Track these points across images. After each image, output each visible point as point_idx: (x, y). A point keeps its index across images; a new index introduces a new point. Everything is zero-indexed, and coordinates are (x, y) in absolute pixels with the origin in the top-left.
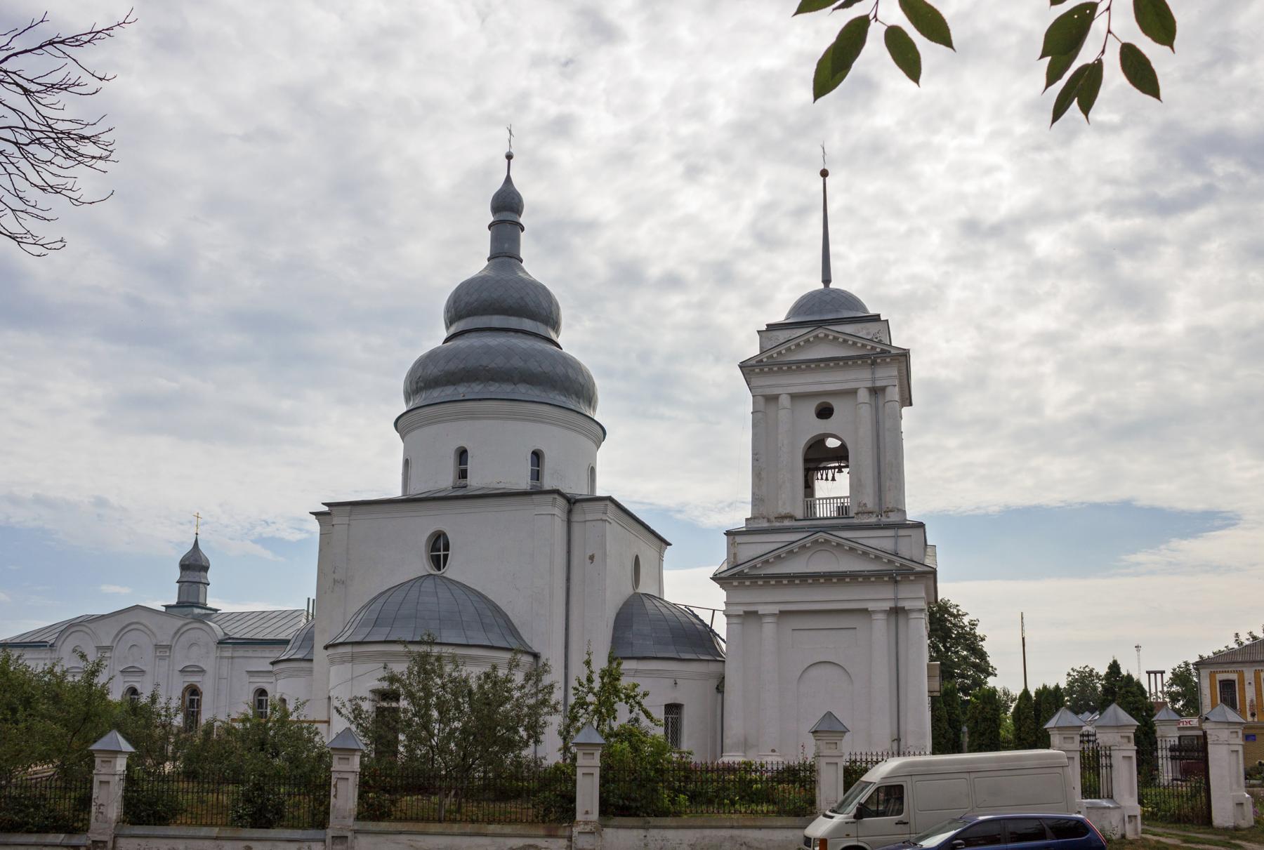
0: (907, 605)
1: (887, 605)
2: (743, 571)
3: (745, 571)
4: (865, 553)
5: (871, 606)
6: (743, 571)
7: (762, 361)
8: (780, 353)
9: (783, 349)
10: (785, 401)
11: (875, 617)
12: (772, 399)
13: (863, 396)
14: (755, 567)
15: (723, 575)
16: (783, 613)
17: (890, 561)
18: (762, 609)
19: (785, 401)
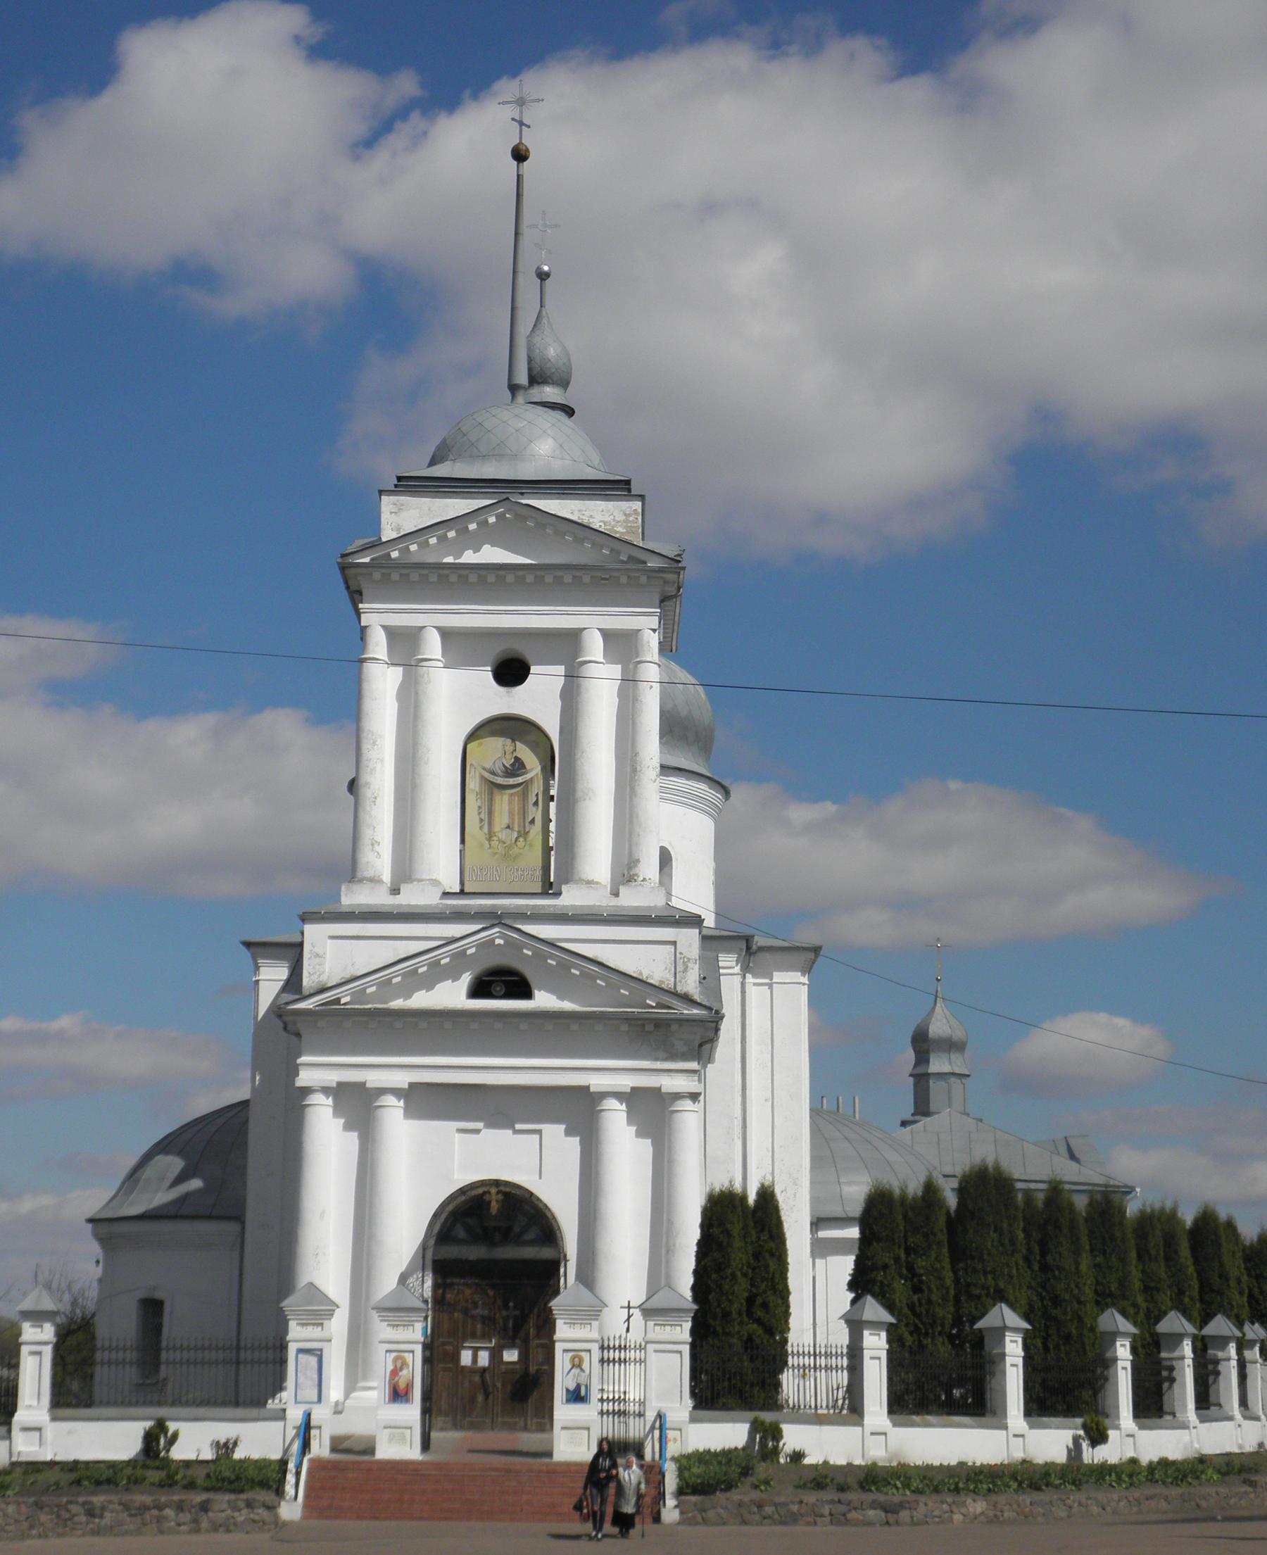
6: (339, 999)
19: (433, 646)
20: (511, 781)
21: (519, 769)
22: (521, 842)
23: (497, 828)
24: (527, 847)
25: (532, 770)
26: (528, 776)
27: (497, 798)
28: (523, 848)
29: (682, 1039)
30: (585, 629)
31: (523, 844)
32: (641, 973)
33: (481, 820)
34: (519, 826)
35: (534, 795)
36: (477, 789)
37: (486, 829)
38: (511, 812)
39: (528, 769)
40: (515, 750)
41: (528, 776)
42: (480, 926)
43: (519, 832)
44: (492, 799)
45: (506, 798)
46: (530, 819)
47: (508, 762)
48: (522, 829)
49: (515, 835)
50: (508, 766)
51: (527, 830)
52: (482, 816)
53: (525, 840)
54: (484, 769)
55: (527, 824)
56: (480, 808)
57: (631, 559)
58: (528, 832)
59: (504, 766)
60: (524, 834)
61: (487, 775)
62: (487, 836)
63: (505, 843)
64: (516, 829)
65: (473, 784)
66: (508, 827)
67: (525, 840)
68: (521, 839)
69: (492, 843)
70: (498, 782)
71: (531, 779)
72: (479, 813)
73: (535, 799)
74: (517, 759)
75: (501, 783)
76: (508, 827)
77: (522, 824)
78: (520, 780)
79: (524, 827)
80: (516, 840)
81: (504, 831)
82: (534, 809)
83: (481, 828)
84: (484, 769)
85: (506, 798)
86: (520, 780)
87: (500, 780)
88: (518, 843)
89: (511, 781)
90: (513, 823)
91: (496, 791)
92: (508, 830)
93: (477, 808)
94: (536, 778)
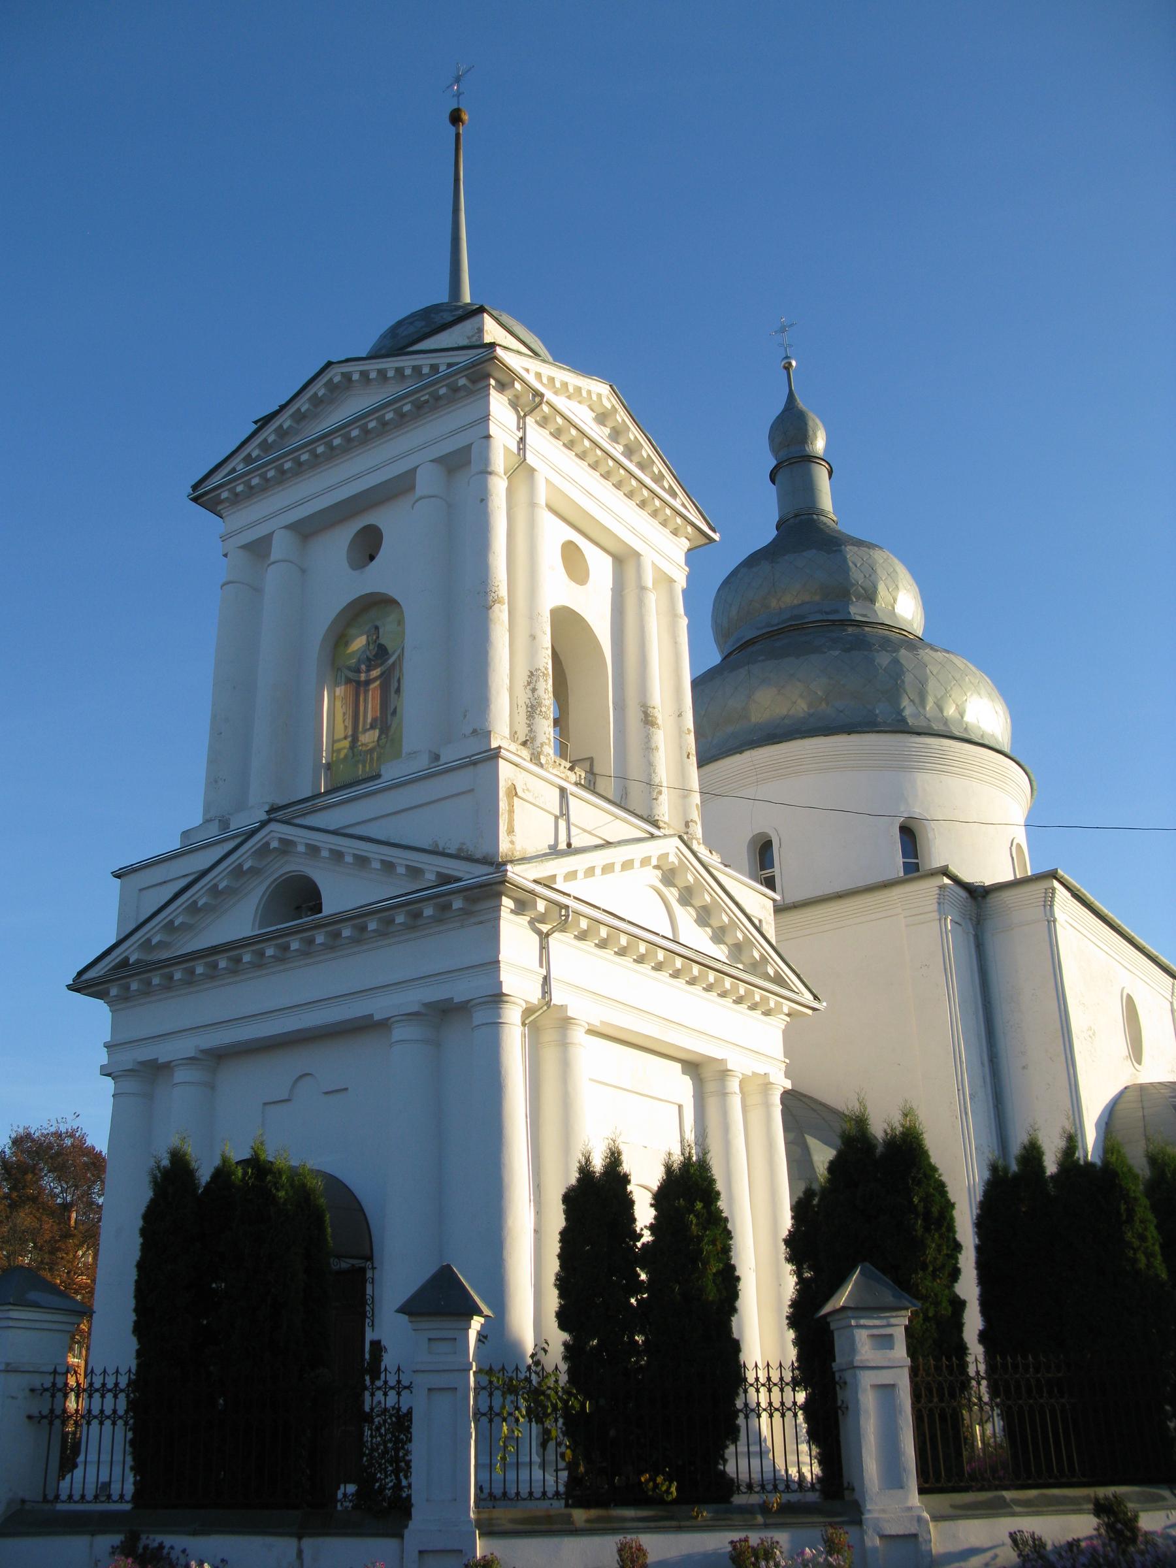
0: (460, 990)
1: (412, 999)
2: (127, 959)
4: (362, 861)
5: (378, 1007)
6: (127, 959)
7: (234, 470)
8: (265, 446)
9: (269, 434)
10: (282, 545)
11: (398, 1033)
12: (259, 549)
13: (428, 480)
14: (147, 945)
15: (91, 974)
16: (219, 1057)
17: (415, 872)
18: (164, 1052)
19: (282, 545)
25: (394, 653)
26: (391, 661)
30: (418, 467)
32: (437, 845)
35: (396, 679)
36: (342, 694)
39: (390, 651)
40: (378, 637)
46: (392, 709)
52: (347, 724)
53: (387, 737)
55: (389, 717)
56: (344, 714)
57: (450, 365)
58: (391, 724)
67: (387, 737)
68: (383, 736)
71: (394, 664)
72: (344, 722)
73: (396, 684)
79: (387, 718)
88: (381, 742)
93: (341, 715)
94: (398, 662)
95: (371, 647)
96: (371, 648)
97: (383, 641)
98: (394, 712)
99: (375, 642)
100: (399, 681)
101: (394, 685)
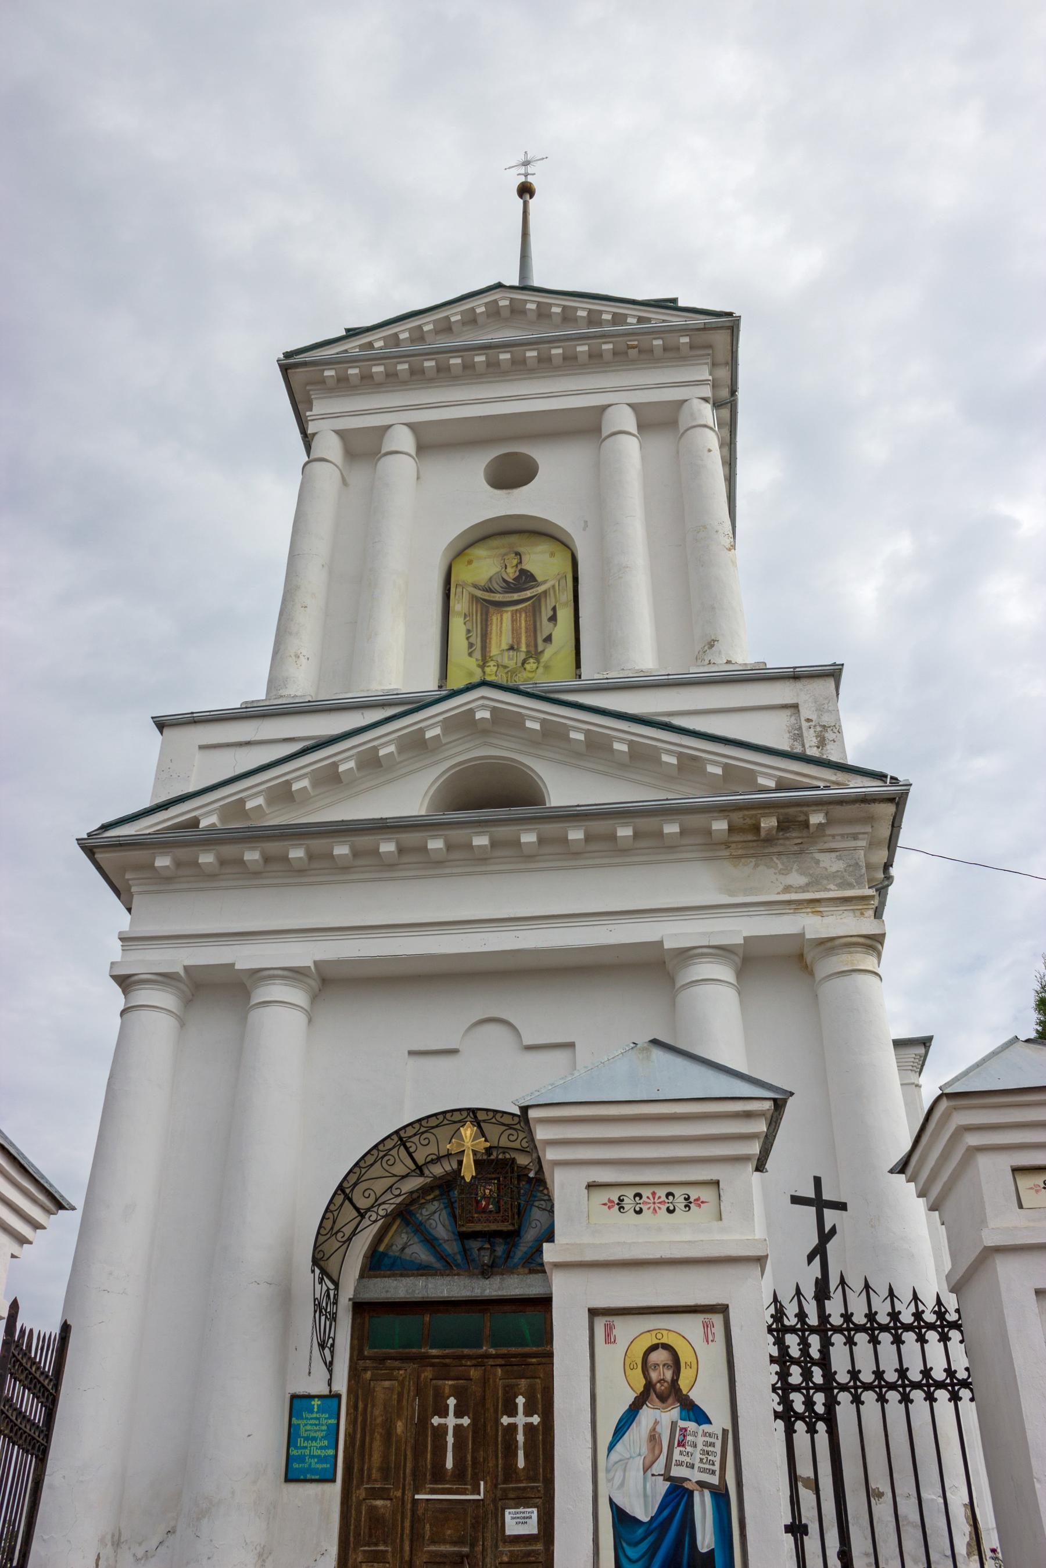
3: (203, 824)
20: (516, 596)
21: (525, 582)
22: (531, 665)
23: (494, 651)
24: (541, 670)
25: (545, 582)
27: (495, 619)
28: (535, 671)
29: (832, 850)
31: (535, 666)
33: (471, 645)
34: (527, 646)
35: (550, 608)
37: (478, 654)
38: (515, 632)
39: (539, 579)
40: (521, 562)
41: (541, 589)
42: (462, 736)
43: (528, 652)
44: (487, 620)
45: (507, 617)
46: (544, 637)
47: (511, 574)
48: (532, 649)
49: (523, 656)
50: (511, 581)
51: (540, 649)
52: (472, 640)
53: (538, 662)
54: (475, 586)
56: (468, 631)
58: (542, 652)
59: (504, 580)
60: (534, 654)
61: (479, 594)
62: (481, 663)
63: (505, 667)
64: (523, 648)
65: (459, 606)
66: (512, 648)
68: (531, 660)
69: (487, 670)
70: (497, 599)
71: (545, 592)
73: (551, 613)
74: (523, 572)
75: (501, 599)
76: (512, 648)
77: (532, 643)
78: (528, 594)
79: (536, 646)
80: (524, 662)
81: (506, 654)
82: (551, 625)
83: (470, 655)
84: (475, 586)
85: (507, 617)
86: (528, 594)
87: (498, 597)
88: (527, 666)
89: (516, 596)
90: (519, 643)
91: (492, 609)
92: (511, 653)
95: (510, 570)
96: (510, 570)
97: (527, 566)
98: (548, 639)
99: (517, 566)
100: (554, 609)
101: (546, 613)
